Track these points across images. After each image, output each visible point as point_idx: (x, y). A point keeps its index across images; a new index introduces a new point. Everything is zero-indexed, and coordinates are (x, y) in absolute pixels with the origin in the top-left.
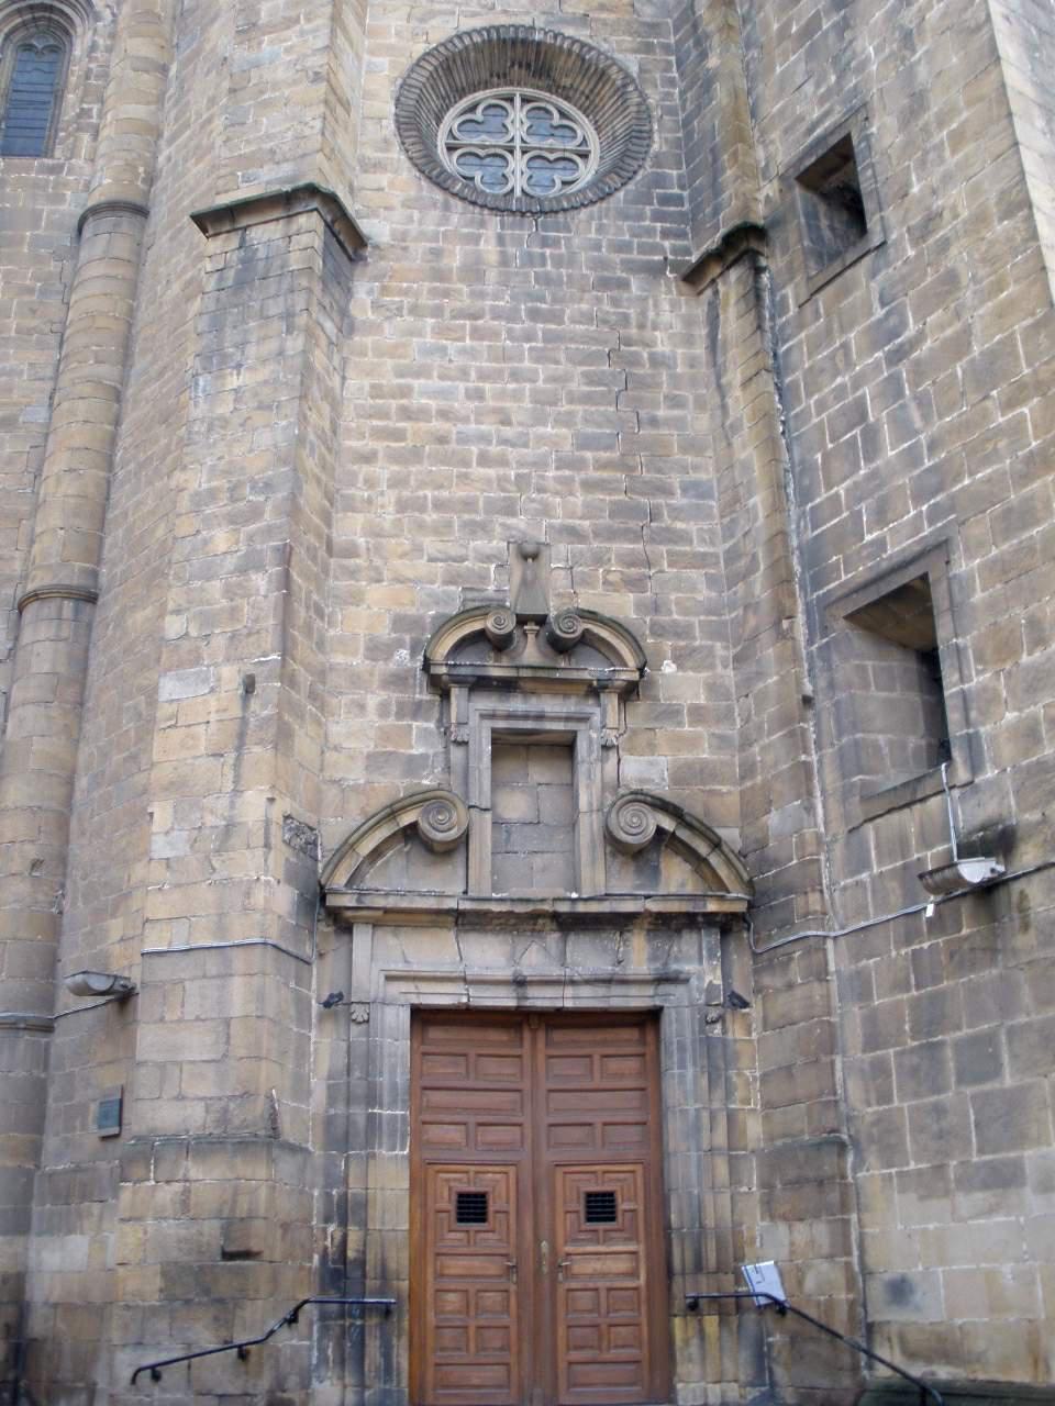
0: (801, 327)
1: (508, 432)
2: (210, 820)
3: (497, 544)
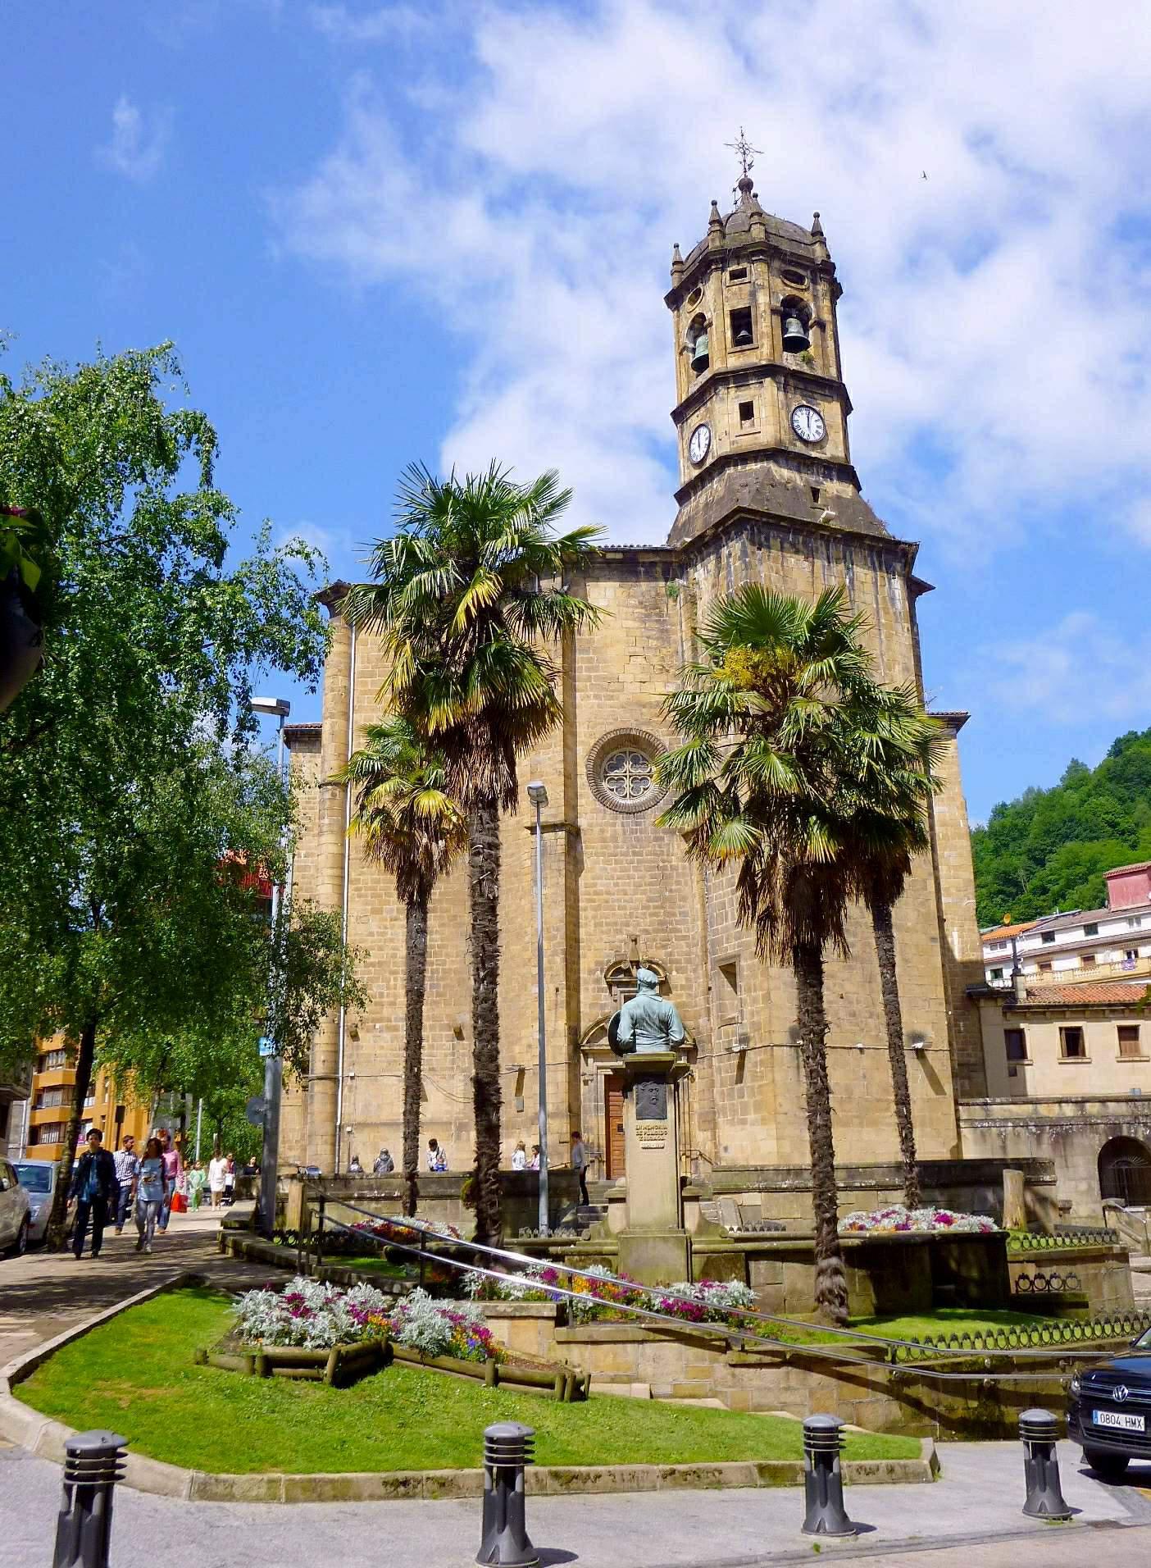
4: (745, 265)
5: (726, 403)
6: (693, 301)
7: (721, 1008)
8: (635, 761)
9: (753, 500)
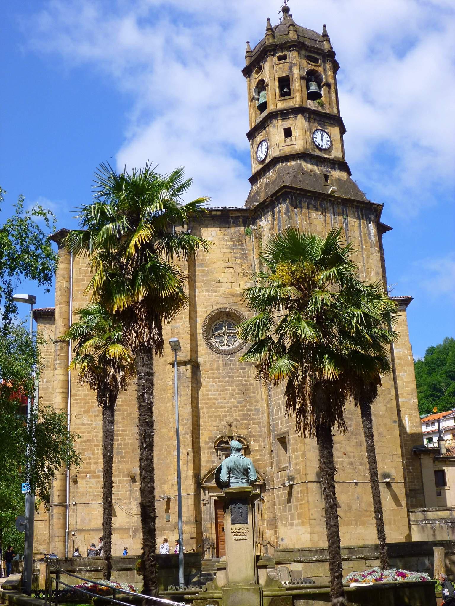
1: (225, 401)
3: (224, 423)
5: (276, 130)
6: (257, 72)
7: (278, 462)
8: (229, 326)
9: (292, 181)
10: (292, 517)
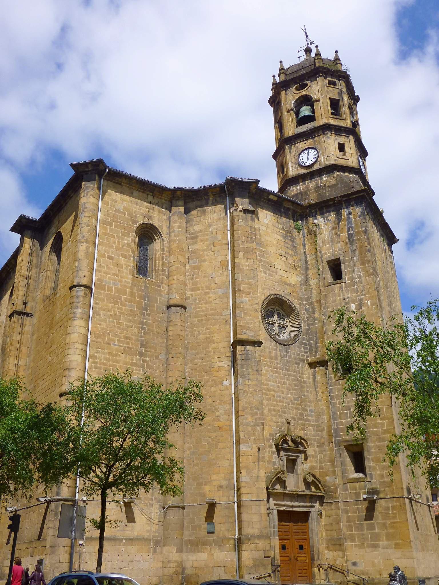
0: (336, 385)
1: (284, 396)
2: (254, 475)
4: (337, 81)
10: (376, 537)
